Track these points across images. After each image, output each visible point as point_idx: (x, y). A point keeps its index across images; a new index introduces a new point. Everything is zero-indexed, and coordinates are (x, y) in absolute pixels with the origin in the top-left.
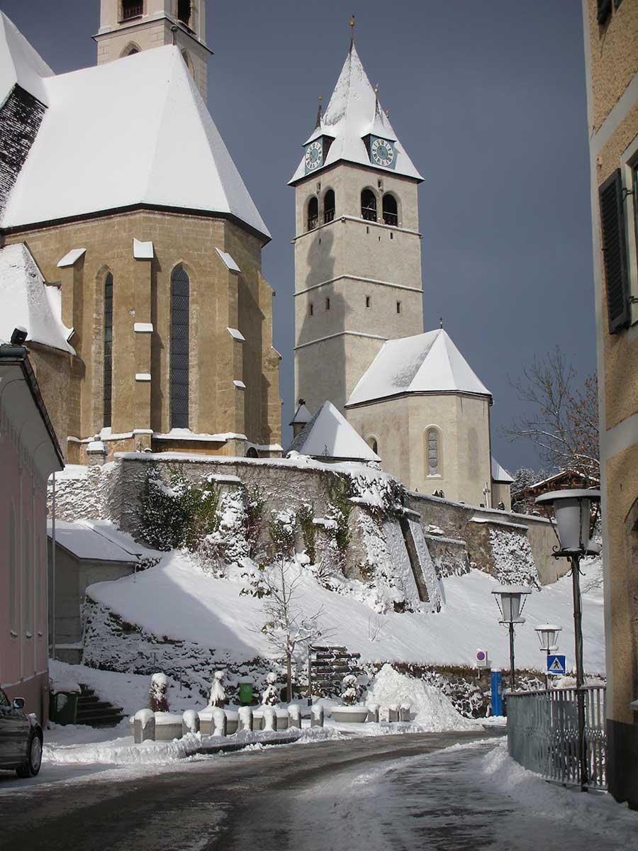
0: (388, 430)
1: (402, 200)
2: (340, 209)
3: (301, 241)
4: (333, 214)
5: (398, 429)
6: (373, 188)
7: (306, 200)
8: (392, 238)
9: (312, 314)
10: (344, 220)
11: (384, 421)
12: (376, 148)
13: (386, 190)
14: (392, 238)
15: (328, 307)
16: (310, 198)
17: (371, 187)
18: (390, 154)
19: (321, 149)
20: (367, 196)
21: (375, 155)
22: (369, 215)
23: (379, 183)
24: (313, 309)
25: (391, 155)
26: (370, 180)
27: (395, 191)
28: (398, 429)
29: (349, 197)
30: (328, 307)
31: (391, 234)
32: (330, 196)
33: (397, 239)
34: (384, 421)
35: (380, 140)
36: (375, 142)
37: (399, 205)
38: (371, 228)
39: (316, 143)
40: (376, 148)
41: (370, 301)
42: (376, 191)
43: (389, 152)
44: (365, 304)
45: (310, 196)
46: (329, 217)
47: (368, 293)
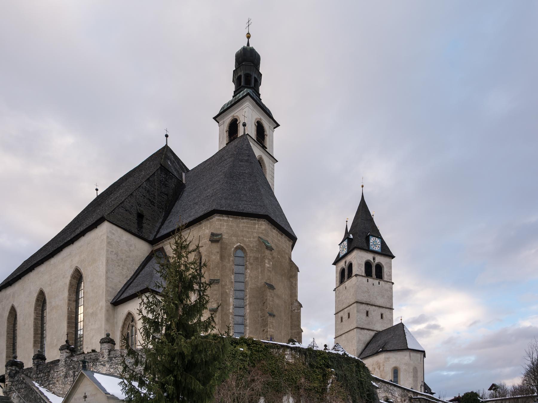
0: (375, 369)
1: (385, 267)
2: (355, 271)
3: (338, 289)
4: (352, 274)
5: (379, 369)
6: (371, 261)
7: (340, 270)
8: (379, 284)
9: (342, 321)
10: (356, 275)
11: (373, 365)
12: (372, 242)
13: (377, 261)
14: (379, 284)
15: (349, 317)
16: (342, 269)
17: (370, 260)
18: (379, 245)
19: (347, 244)
20: (368, 265)
21: (372, 245)
22: (368, 273)
23: (374, 259)
24: (343, 319)
25: (379, 245)
26: (369, 257)
27: (381, 262)
28: (379, 369)
29: (359, 265)
30: (349, 317)
31: (379, 282)
32: (350, 266)
33: (382, 285)
34: (373, 365)
35: (374, 238)
36: (372, 239)
37: (383, 269)
38: (370, 280)
39: (344, 242)
40: (372, 242)
41: (368, 313)
42: (372, 262)
43: (379, 243)
44: (365, 315)
45: (342, 268)
46: (350, 276)
47: (367, 310)
